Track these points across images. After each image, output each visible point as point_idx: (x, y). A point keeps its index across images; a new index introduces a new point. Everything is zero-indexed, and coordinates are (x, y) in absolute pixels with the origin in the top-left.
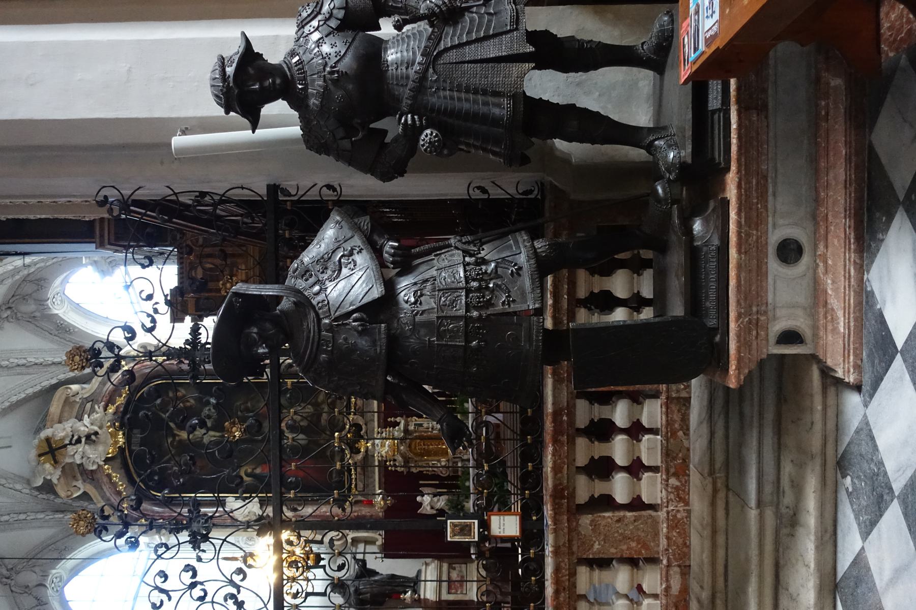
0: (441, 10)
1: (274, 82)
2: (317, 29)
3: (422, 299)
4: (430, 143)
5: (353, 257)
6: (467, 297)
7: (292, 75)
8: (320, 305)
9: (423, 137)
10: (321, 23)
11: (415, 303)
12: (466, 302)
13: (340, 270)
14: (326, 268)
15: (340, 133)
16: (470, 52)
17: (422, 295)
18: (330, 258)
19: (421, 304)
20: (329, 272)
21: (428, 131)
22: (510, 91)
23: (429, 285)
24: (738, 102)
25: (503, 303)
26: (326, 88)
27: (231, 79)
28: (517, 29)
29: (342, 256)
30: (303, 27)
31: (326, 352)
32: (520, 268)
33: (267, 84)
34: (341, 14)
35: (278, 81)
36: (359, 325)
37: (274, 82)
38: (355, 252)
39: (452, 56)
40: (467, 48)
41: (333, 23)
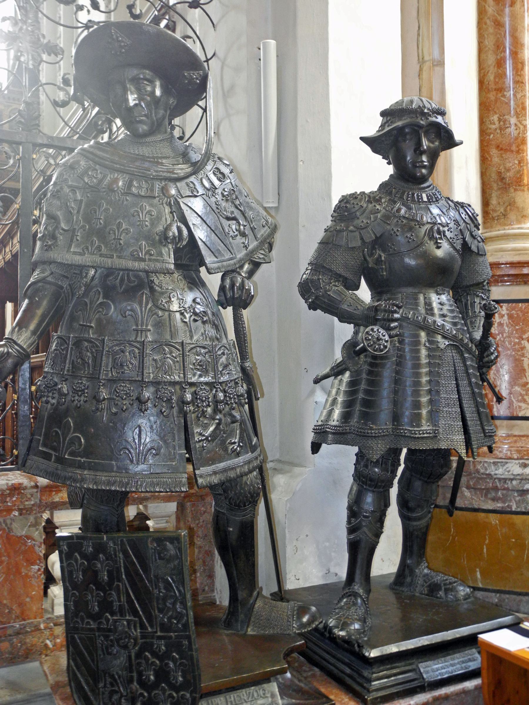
0: (492, 353)
1: (424, 167)
2: (464, 221)
3: (199, 323)
4: (379, 339)
5: (239, 237)
6: (206, 384)
7: (424, 188)
8: (192, 185)
9: (382, 331)
10: (468, 226)
11: (195, 314)
12: (201, 383)
13: (228, 219)
14: (227, 200)
15: (369, 237)
16: (464, 383)
17: (204, 322)
18: (236, 207)
19: (195, 321)
20: (224, 204)
21: (387, 337)
22: (438, 433)
23: (212, 332)
24: (436, 699)
25: (201, 434)
26: (421, 224)
27: (434, 119)
28: (485, 436)
29: (239, 223)
30: (462, 207)
31: (130, 185)
32: (238, 455)
33: (424, 158)
34: (474, 248)
35: (424, 171)
36: (174, 233)
37: (424, 167)
38: (243, 240)
39: (460, 366)
40: (466, 382)
41: (468, 238)
